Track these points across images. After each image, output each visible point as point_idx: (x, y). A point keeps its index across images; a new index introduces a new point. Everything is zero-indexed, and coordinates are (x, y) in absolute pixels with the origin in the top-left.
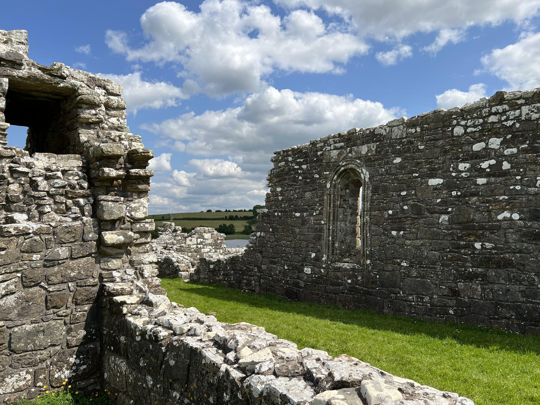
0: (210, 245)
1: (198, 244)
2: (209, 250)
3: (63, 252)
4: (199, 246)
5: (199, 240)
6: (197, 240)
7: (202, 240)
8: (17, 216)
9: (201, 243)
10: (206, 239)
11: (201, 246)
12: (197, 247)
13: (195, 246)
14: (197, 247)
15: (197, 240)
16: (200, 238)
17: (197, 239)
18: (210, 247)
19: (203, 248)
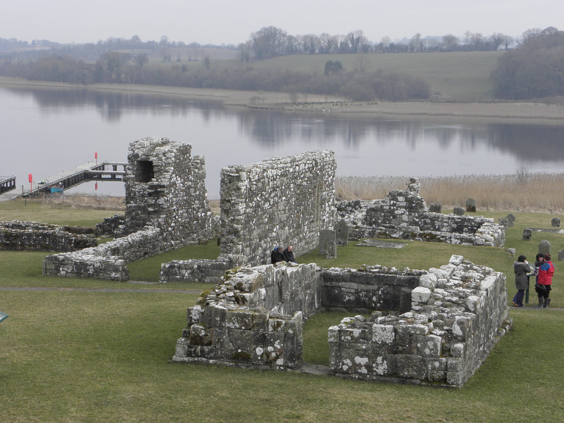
0: (403, 207)
1: (390, 205)
2: (403, 212)
3: (139, 212)
4: (392, 208)
5: (392, 202)
6: (390, 202)
7: (395, 202)
8: (132, 202)
9: (394, 205)
10: (399, 202)
11: (395, 207)
12: (390, 208)
13: (388, 207)
14: (390, 208)
15: (390, 202)
16: (393, 200)
17: (390, 200)
18: (404, 210)
19: (397, 210)
